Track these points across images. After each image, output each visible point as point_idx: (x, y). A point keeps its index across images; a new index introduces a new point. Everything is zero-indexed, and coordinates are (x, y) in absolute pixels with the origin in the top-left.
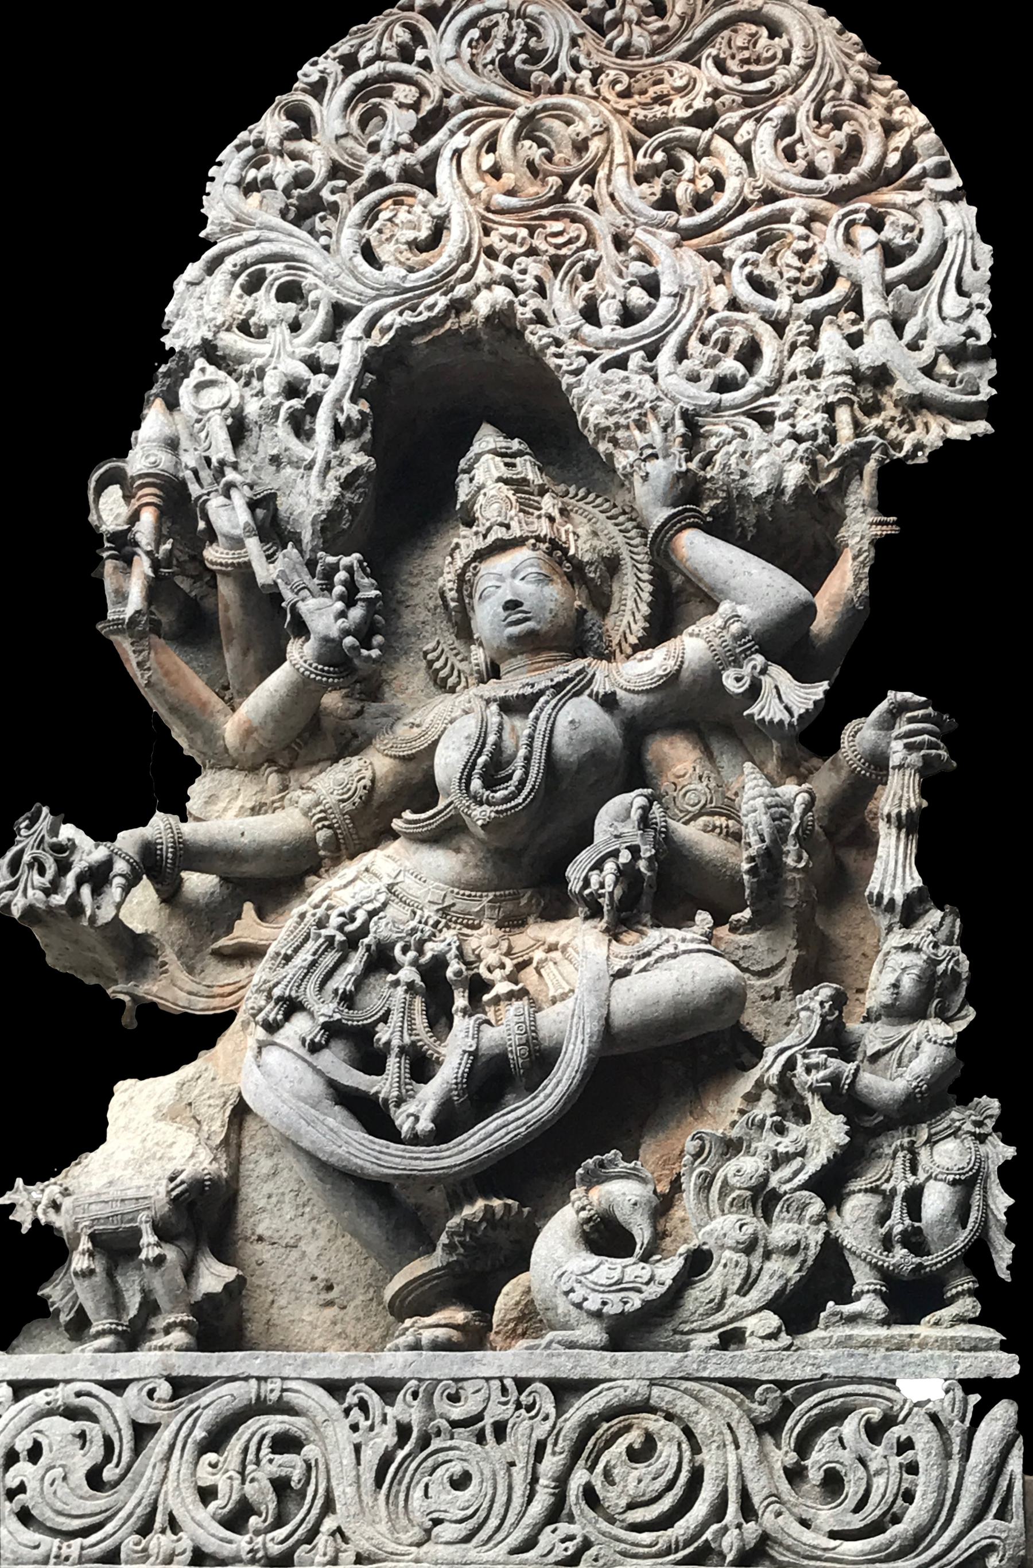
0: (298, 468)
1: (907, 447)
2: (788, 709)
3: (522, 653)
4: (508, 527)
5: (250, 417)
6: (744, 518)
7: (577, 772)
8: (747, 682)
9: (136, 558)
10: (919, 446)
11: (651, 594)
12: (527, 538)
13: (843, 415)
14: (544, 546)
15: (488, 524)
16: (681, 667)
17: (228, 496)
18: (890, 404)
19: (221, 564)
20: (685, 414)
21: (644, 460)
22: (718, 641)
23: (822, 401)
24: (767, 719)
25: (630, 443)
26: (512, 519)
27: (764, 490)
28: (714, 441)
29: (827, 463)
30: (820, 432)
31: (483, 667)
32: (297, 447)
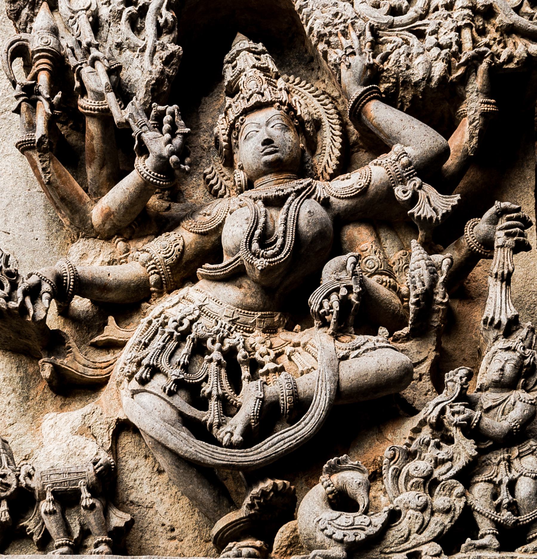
0: (134, 51)
1: (504, 57)
2: (435, 210)
3: (271, 173)
4: (263, 95)
5: (103, 17)
6: (404, 97)
7: (311, 242)
8: (410, 194)
9: (39, 102)
10: (511, 58)
11: (341, 144)
12: (274, 102)
13: (466, 34)
14: (285, 108)
15: (251, 92)
16: (369, 183)
17: (93, 66)
18: (493, 30)
19: (91, 109)
20: (372, 28)
21: (348, 56)
22: (393, 168)
23: (454, 24)
24: (423, 216)
25: (338, 45)
26: (265, 90)
27: (420, 77)
28: (388, 47)
29: (457, 64)
30: (454, 44)
31: (243, 183)
32: (134, 39)
